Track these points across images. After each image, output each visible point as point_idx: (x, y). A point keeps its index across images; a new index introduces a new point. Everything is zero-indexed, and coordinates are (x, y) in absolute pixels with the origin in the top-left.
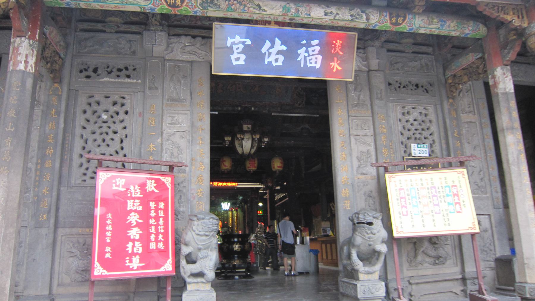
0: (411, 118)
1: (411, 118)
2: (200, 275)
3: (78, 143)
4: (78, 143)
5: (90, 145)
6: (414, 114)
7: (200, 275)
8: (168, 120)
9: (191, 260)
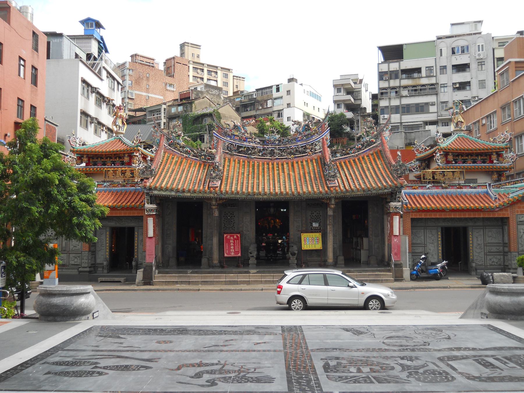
0: (314, 215)
1: (314, 215)
2: (253, 256)
3: (223, 225)
4: (223, 225)
5: (226, 225)
6: (315, 214)
7: (253, 256)
8: (244, 218)
9: (251, 253)
